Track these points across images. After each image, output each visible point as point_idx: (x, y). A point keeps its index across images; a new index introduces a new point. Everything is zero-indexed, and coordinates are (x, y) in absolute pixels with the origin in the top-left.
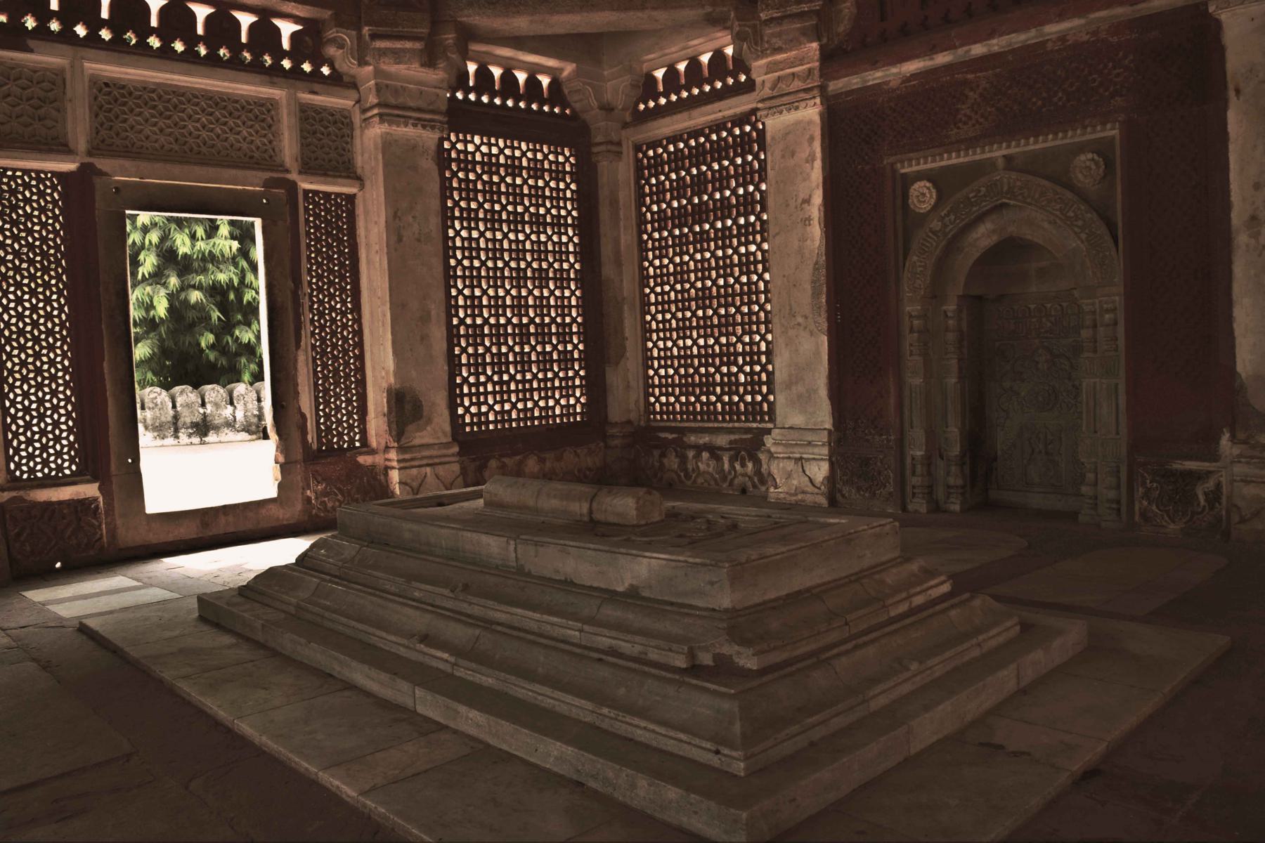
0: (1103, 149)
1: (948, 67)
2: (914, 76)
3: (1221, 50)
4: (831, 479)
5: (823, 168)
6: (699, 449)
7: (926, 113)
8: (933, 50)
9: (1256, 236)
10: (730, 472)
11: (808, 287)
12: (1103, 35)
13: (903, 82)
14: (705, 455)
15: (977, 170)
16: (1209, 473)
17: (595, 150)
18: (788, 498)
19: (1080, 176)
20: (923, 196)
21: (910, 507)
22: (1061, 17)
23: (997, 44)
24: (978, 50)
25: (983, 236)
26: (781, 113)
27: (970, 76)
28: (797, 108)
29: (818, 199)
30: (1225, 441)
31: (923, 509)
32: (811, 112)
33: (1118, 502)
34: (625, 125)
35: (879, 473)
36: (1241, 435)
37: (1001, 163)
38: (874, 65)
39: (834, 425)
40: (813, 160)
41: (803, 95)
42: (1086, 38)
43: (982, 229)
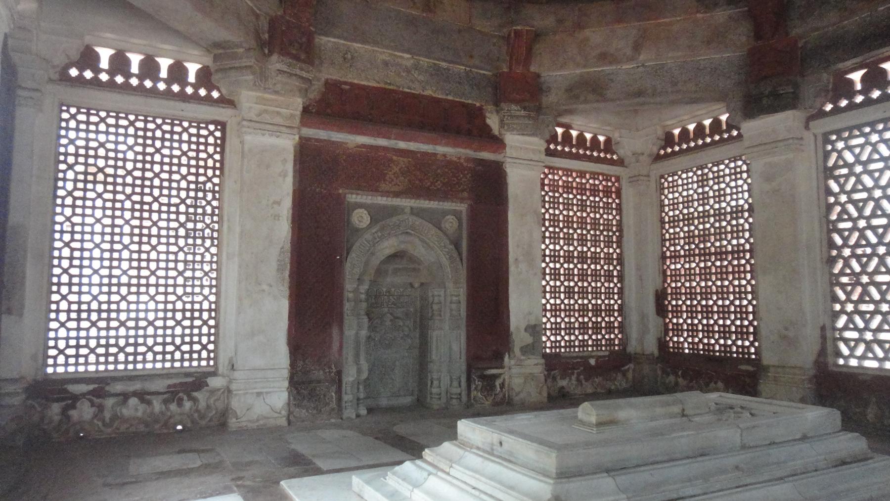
0: (456, 214)
1: (385, 149)
2: (363, 146)
3: (506, 184)
4: (289, 404)
5: (294, 184)
6: (125, 397)
7: (368, 170)
8: (379, 135)
9: (517, 267)
10: (162, 413)
11: (274, 265)
12: (462, 161)
13: (357, 147)
14: (133, 401)
15: (395, 211)
16: (501, 374)
17: (20, 92)
18: (250, 425)
19: (447, 226)
20: (360, 218)
21: (344, 417)
22: (447, 145)
23: (412, 146)
24: (402, 145)
25: (388, 246)
26: (263, 135)
27: (395, 158)
28: (278, 137)
29: (287, 203)
30: (506, 359)
31: (354, 416)
32: (287, 143)
33: (460, 394)
34: (51, 80)
35: (325, 396)
36: (512, 356)
37: (408, 210)
38: (340, 129)
39: (291, 365)
40: (285, 176)
41: (284, 129)
42: (455, 159)
43: (386, 244)
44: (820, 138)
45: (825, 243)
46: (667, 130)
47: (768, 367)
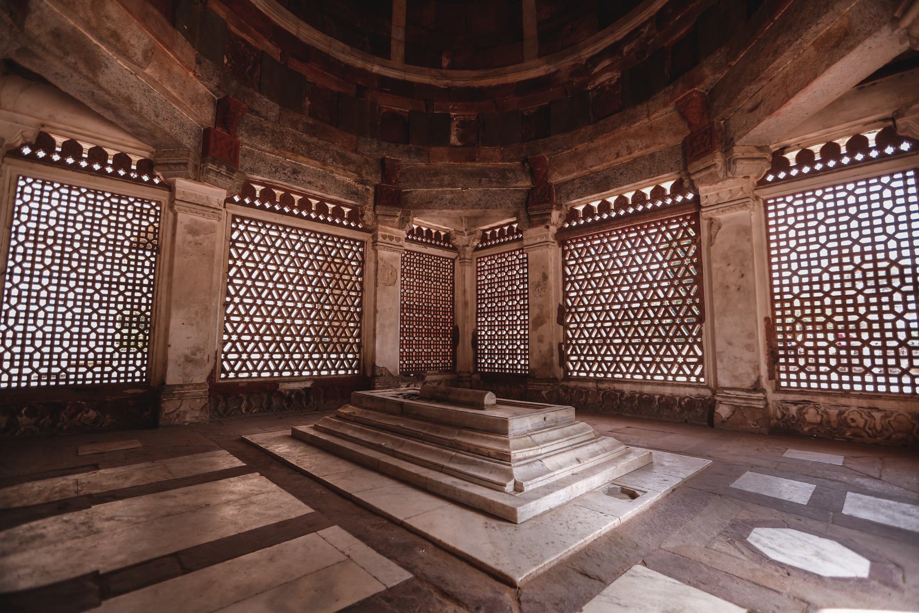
44: (230, 218)
45: (224, 292)
46: (42, 129)
47: (173, 386)
